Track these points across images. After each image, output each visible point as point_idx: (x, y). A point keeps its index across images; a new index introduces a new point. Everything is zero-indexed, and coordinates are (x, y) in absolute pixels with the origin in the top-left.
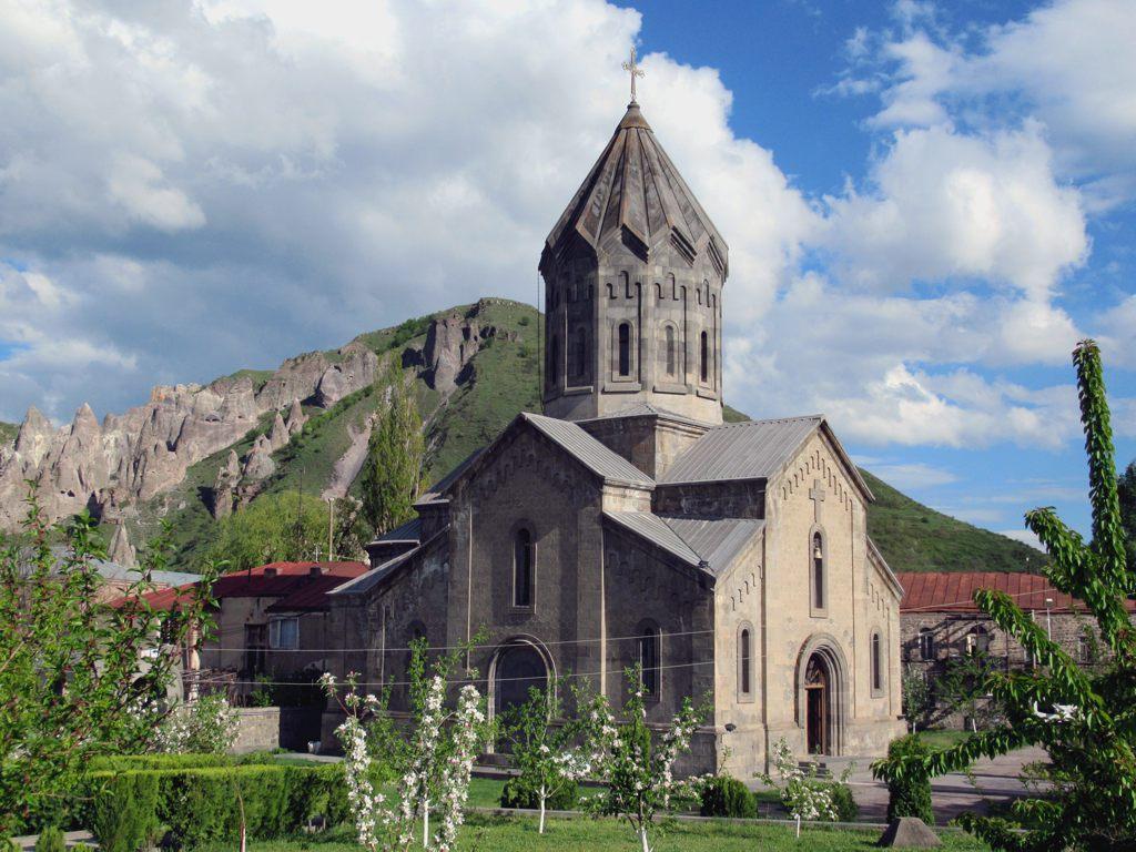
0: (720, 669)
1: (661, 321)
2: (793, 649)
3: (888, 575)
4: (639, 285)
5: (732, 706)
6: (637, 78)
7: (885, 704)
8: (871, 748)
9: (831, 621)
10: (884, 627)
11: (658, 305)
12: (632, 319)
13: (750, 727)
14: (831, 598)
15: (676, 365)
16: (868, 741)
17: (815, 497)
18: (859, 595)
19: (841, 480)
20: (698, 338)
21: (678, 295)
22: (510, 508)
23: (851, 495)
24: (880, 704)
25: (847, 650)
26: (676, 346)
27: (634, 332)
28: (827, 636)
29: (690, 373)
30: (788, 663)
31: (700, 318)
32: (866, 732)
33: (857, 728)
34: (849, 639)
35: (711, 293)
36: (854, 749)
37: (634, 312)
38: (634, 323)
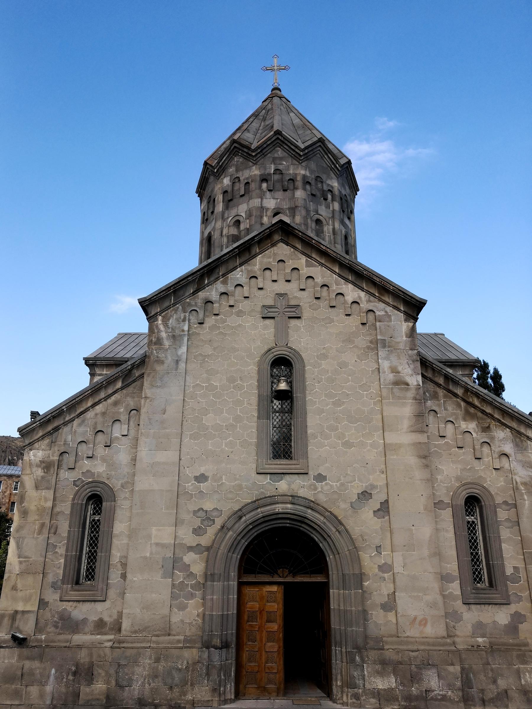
5: (43, 604)
8: (444, 698)
9: (320, 478)
13: (78, 638)
24: (502, 617)
28: (294, 499)
32: (427, 664)
33: (389, 654)
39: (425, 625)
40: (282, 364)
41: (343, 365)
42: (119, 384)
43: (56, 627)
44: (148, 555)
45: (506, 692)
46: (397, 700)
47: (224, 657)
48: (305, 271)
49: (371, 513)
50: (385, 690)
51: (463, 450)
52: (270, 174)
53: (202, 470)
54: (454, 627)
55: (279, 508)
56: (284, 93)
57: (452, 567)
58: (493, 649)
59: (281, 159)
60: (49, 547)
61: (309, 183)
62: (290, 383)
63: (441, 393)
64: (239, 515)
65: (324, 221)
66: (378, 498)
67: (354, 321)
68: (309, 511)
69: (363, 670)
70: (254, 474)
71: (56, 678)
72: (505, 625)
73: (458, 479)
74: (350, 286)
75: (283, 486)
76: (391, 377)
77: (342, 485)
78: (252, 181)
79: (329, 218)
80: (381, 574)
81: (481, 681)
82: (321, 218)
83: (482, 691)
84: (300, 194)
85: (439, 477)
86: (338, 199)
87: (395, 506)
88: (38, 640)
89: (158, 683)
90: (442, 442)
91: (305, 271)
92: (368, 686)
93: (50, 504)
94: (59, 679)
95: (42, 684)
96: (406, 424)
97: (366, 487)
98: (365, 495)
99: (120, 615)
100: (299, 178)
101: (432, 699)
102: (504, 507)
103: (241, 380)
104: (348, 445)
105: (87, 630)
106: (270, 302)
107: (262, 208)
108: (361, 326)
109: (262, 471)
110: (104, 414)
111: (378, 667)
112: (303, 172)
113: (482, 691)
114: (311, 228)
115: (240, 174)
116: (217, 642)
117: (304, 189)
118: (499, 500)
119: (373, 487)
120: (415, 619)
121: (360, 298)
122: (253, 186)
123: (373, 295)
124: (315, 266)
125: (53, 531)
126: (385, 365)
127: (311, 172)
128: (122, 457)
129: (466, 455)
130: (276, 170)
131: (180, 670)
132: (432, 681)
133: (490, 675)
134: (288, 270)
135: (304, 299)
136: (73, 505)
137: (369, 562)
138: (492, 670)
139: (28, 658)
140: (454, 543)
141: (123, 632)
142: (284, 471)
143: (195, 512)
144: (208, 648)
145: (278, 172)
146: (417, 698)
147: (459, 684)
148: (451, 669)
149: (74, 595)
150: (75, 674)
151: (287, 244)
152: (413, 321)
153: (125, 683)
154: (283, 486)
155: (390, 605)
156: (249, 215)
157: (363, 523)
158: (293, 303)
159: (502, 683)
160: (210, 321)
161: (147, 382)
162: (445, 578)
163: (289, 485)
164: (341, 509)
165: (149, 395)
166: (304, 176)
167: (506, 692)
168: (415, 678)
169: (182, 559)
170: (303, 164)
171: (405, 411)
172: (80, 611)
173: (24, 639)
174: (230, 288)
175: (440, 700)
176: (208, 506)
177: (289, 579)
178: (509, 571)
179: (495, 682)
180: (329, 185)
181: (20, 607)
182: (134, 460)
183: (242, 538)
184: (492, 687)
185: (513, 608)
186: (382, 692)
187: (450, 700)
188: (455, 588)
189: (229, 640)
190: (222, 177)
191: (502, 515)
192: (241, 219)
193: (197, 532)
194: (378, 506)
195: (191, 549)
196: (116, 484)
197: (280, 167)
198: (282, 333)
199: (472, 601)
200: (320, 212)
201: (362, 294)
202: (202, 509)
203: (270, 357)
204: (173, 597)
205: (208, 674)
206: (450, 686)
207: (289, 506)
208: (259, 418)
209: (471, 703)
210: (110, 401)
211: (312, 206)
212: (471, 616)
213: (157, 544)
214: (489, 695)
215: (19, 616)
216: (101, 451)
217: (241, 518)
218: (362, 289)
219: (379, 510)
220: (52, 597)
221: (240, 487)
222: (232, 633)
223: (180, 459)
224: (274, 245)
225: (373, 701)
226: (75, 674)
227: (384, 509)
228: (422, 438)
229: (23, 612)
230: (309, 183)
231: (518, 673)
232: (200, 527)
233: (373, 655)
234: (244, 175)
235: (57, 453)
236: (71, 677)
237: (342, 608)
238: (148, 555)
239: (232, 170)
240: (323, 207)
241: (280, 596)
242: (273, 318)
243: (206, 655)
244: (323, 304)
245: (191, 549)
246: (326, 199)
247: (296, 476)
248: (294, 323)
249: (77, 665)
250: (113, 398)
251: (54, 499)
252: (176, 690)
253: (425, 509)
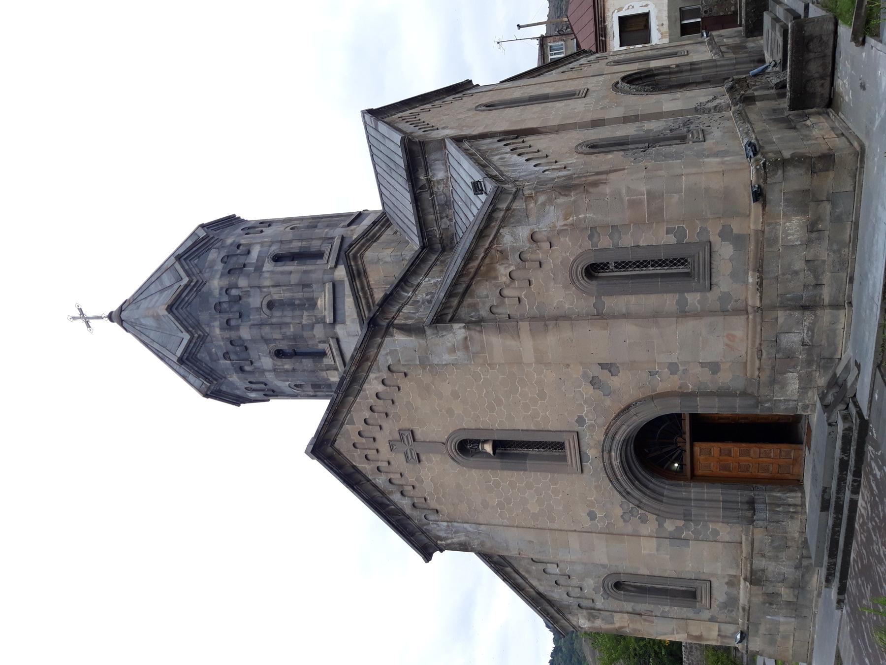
5: (712, 620)
7: (726, 234)
9: (580, 421)
10: (570, 250)
24: (725, 251)
28: (605, 450)
33: (765, 377)
34: (604, 375)
36: (806, 384)
39: (734, 336)
40: (466, 447)
41: (455, 395)
42: (509, 569)
43: (732, 611)
44: (668, 557)
45: (807, 261)
46: (811, 372)
47: (762, 506)
48: (361, 426)
49: (615, 379)
50: (800, 383)
51: (532, 279)
52: (233, 365)
53: (584, 515)
54: (736, 301)
55: (616, 463)
56: (115, 307)
57: (669, 301)
58: (760, 269)
59: (210, 353)
60: (663, 616)
61: (228, 322)
62: (485, 441)
63: (468, 301)
64: (626, 494)
65: (268, 299)
66: (597, 371)
67: (404, 383)
68: (617, 437)
69: (780, 401)
70: (585, 475)
71: (774, 615)
72: (735, 248)
73: (566, 287)
74: (366, 386)
75: (592, 453)
76: (460, 354)
77: (585, 402)
79: (261, 292)
80: (680, 373)
81: (795, 287)
82: (265, 303)
83: (805, 286)
84: (245, 333)
85: (567, 306)
86: (233, 279)
87: (606, 359)
88: (743, 624)
89: (783, 555)
90: (525, 301)
91: (361, 426)
92: (796, 397)
93: (626, 616)
94: (775, 614)
95: (778, 623)
96: (511, 343)
97: (586, 381)
98: (594, 382)
101: (811, 340)
102: (595, 240)
103: (489, 482)
104: (542, 395)
105: (735, 592)
106: (402, 457)
107: (274, 370)
108: (409, 377)
109: (579, 470)
110: (539, 580)
111: (777, 387)
112: (217, 331)
113: (805, 286)
114: (281, 317)
116: (749, 514)
117: (237, 328)
118: (588, 245)
119: (585, 375)
120: (727, 345)
121: (376, 378)
123: (370, 368)
124: (352, 416)
125: (650, 613)
126: (447, 358)
127: (213, 319)
129: (537, 277)
131: (772, 541)
132: (793, 339)
133: (790, 277)
134: (363, 440)
135: (390, 429)
136: (625, 601)
137: (667, 383)
138: (783, 274)
139: (757, 632)
140: (642, 296)
141: (738, 573)
142: (577, 452)
143: (625, 521)
144: (753, 521)
145: (227, 356)
146: (809, 353)
147: (797, 314)
148: (781, 320)
149: (705, 601)
150: (771, 604)
152: (391, 329)
153: (782, 577)
154: (592, 453)
155: (714, 367)
157: (626, 386)
158: (397, 437)
159: (799, 265)
160: (433, 504)
161: (505, 553)
162: (683, 313)
163: (591, 448)
164: (613, 406)
165: (517, 552)
166: (222, 329)
167: (807, 261)
168: (790, 356)
169: (670, 532)
170: (207, 330)
171: (496, 343)
172: (720, 594)
173: (742, 633)
175: (813, 332)
176: (619, 512)
177: (687, 436)
178: (672, 239)
179: (796, 273)
180: (220, 294)
181: (716, 633)
183: (647, 487)
184: (802, 275)
185: (715, 239)
186: (802, 385)
187: (814, 323)
188: (693, 299)
189: (745, 499)
191: (605, 242)
194: (606, 371)
195: (661, 525)
196: (604, 573)
197: (220, 354)
198: (433, 445)
199: (707, 283)
200: (258, 305)
201: (372, 376)
202: (622, 516)
203: (459, 458)
205: (777, 522)
206: (800, 322)
207: (613, 454)
208: (525, 470)
209: (818, 298)
210: (527, 576)
211: (255, 317)
212: (724, 283)
213: (658, 550)
214: (811, 280)
215: (723, 634)
216: (575, 581)
217: (628, 493)
219: (610, 371)
220: (706, 614)
221: (596, 487)
222: (741, 495)
223: (575, 531)
224: (339, 453)
225: (810, 394)
226: (771, 604)
228: (524, 326)
229: (719, 631)
230: (228, 322)
231: (789, 247)
232: (640, 518)
233: (764, 391)
235: (581, 611)
236: (774, 606)
238: (668, 557)
240: (251, 300)
241: (705, 445)
242: (418, 454)
243: (761, 523)
244: (392, 411)
245: (661, 525)
246: (240, 298)
247: (581, 441)
248: (418, 436)
249: (764, 603)
250: (523, 573)
251: (622, 612)
252: (789, 544)
253: (605, 329)
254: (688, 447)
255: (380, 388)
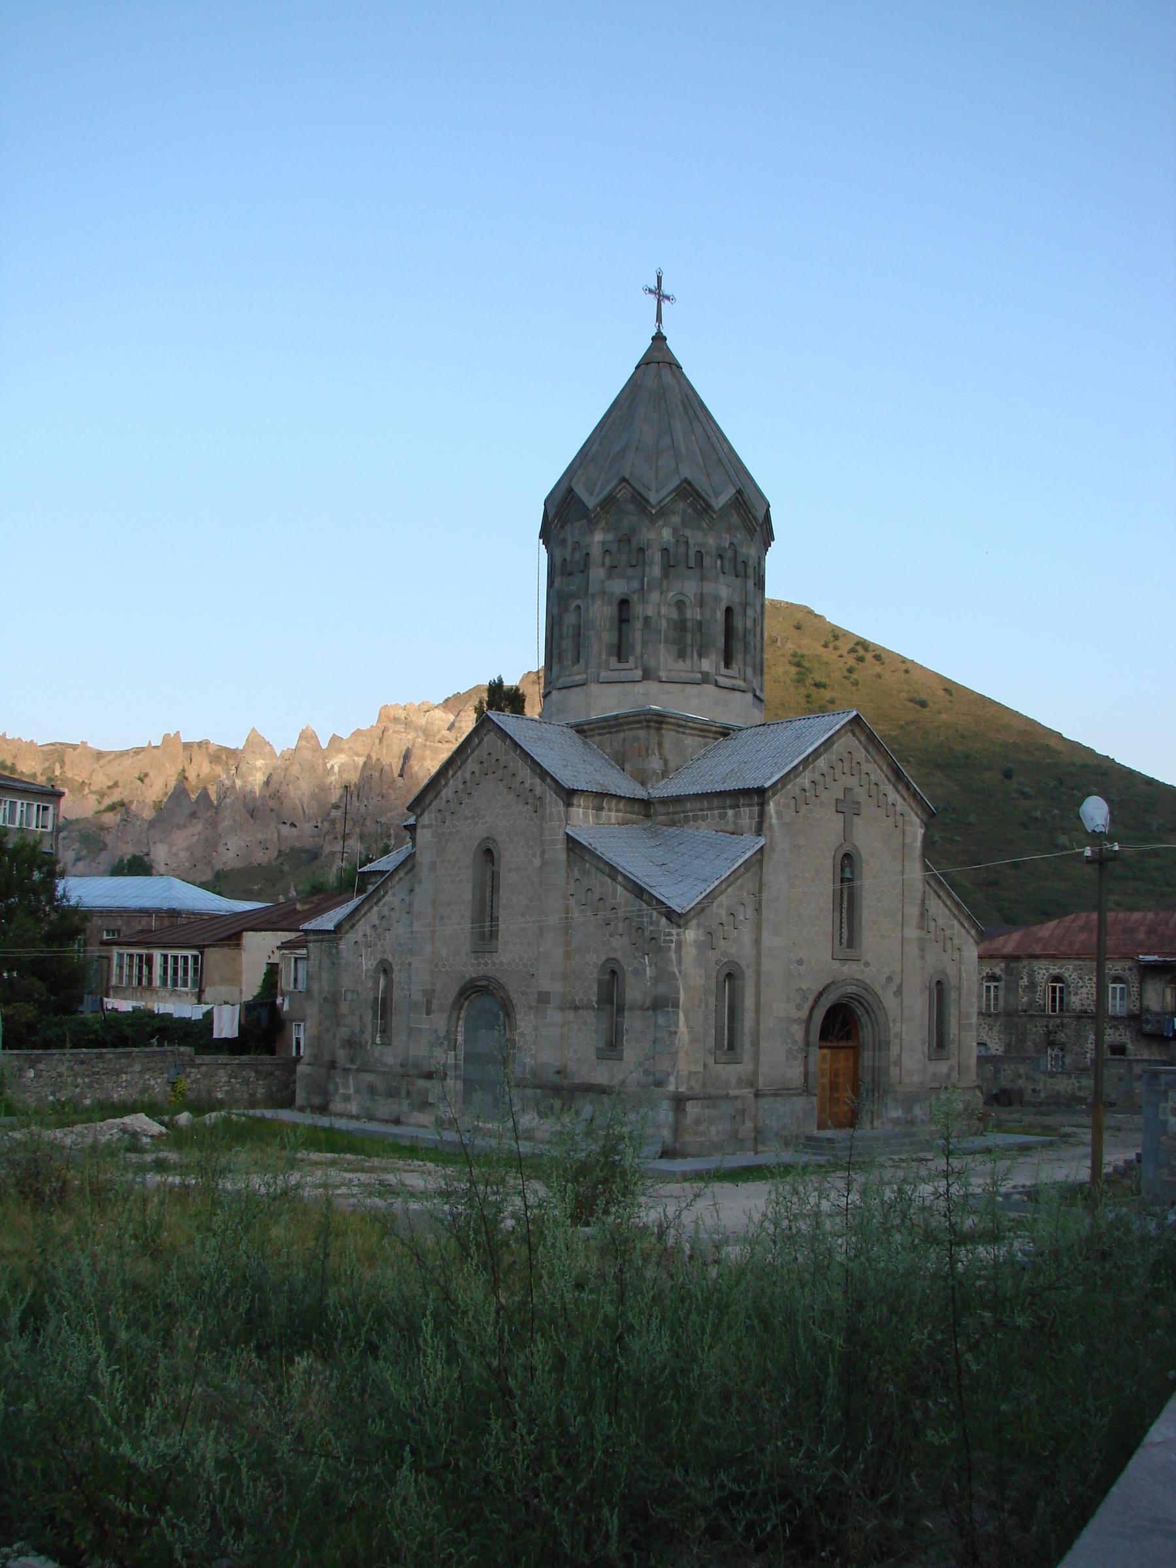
0: (686, 1016)
1: (671, 594)
2: (805, 998)
3: (957, 905)
4: (641, 550)
5: (705, 1066)
6: (665, 305)
7: (951, 1068)
9: (867, 964)
10: (951, 971)
11: (666, 574)
12: (634, 593)
14: (869, 939)
15: (689, 651)
16: (918, 1111)
17: (847, 808)
18: (912, 933)
19: (889, 789)
20: (720, 616)
21: (692, 563)
22: (476, 824)
23: (901, 806)
24: (943, 1067)
25: (889, 1000)
26: (689, 624)
27: (638, 610)
29: (707, 657)
30: (795, 1014)
31: (724, 591)
35: (740, 559)
37: (635, 584)
38: (635, 597)
52: (725, 549)
66: (897, 981)
75: (849, 969)
78: (707, 554)
91: (866, 767)
98: (890, 979)
99: (755, 1073)
100: (751, 563)
115: (688, 533)
122: (707, 561)
128: (747, 940)
130: (732, 544)
139: (708, 1107)
151: (854, 734)
155: (898, 1062)
156: (701, 601)
164: (877, 988)
168: (909, 1110)
174: (817, 777)
176: (804, 987)
181: (692, 1069)
182: (757, 942)
185: (949, 1063)
190: (660, 523)
191: (953, 995)
192: (687, 602)
193: (799, 1007)
197: (735, 541)
204: (787, 1059)
218: (898, 791)
227: (899, 992)
229: (696, 1073)
234: (695, 537)
237: (877, 1064)
239: (676, 520)
245: (795, 1020)
248: (856, 818)
254: (829, 1044)
255: (890, 800)
